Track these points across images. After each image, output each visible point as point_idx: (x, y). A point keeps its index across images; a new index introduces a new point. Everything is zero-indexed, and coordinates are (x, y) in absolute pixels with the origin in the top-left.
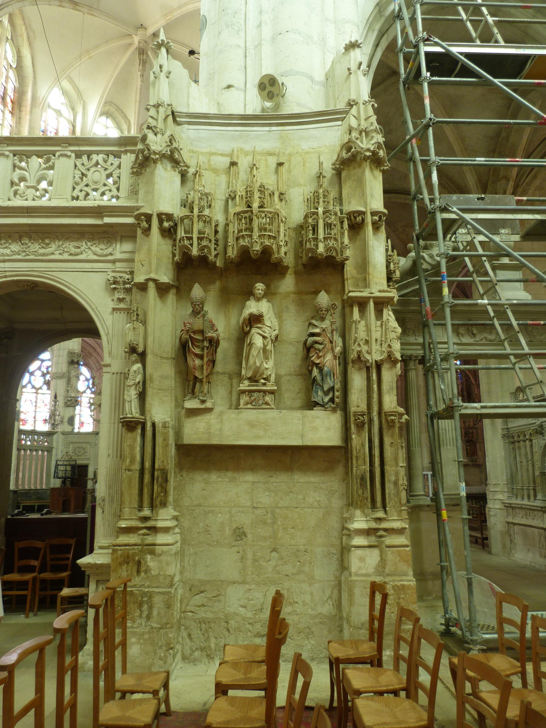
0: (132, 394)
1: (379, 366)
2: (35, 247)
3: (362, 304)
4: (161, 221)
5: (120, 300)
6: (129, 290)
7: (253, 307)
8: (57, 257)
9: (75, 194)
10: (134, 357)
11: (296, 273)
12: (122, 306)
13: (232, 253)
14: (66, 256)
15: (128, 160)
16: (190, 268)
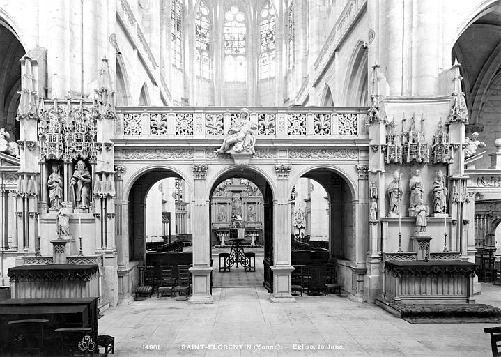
0: (373, 213)
1: (462, 203)
2: (327, 154)
3: (457, 181)
4: (382, 148)
5: (361, 176)
6: (365, 172)
7: (415, 180)
8: (336, 159)
9: (340, 131)
10: (374, 199)
11: (429, 165)
12: (362, 178)
13: (409, 160)
14: (339, 158)
15: (361, 118)
16: (390, 165)
